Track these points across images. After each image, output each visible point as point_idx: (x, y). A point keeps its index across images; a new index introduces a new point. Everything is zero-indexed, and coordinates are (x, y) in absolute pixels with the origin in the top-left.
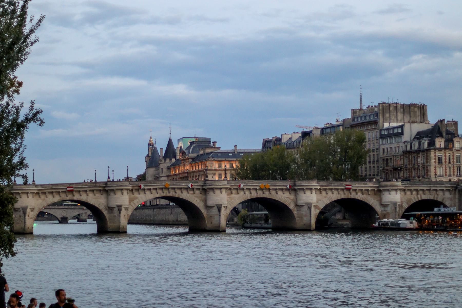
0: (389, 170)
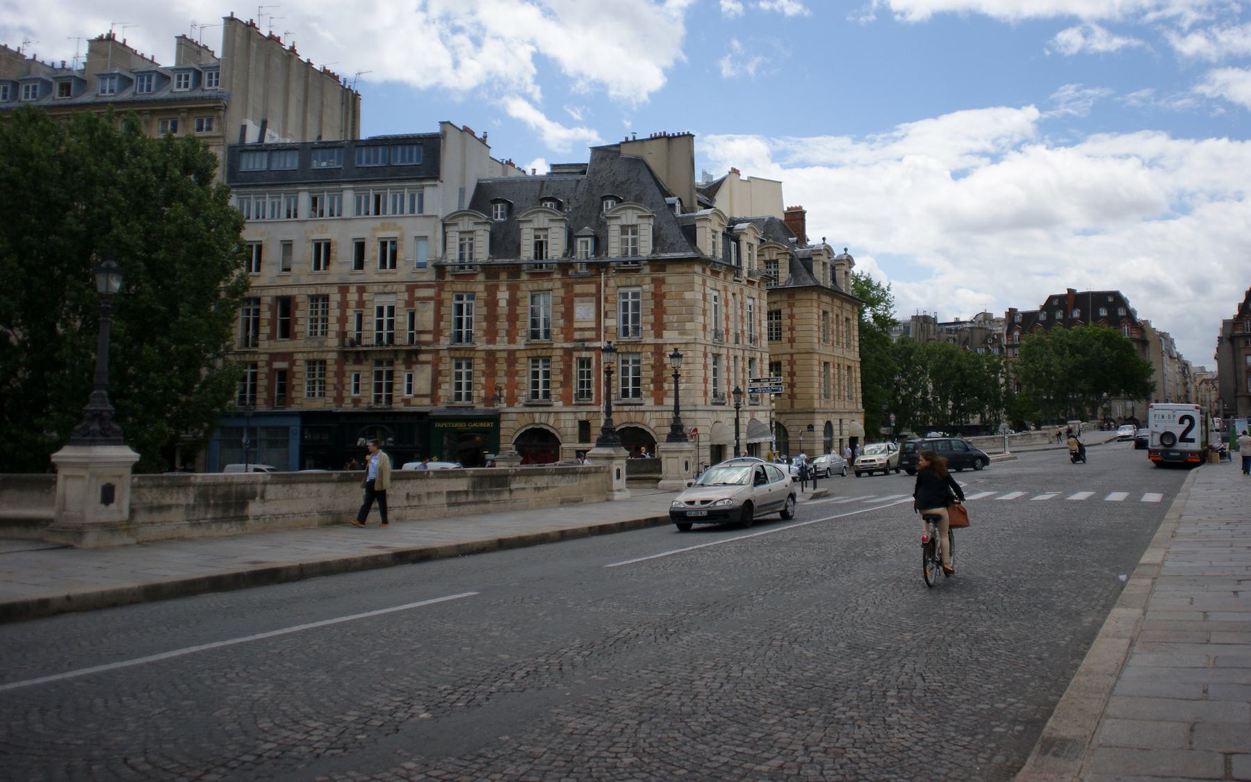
0: (297, 356)
